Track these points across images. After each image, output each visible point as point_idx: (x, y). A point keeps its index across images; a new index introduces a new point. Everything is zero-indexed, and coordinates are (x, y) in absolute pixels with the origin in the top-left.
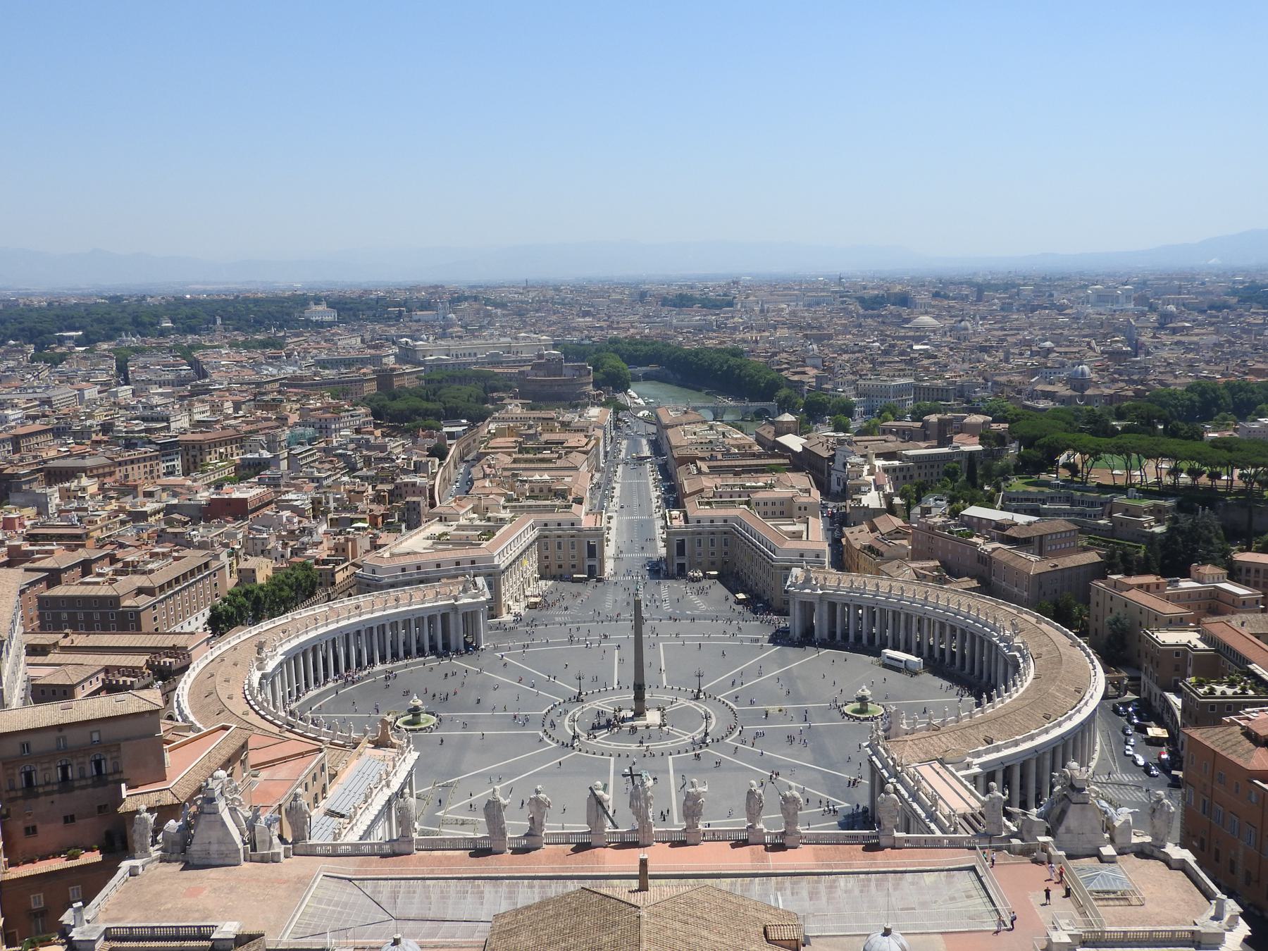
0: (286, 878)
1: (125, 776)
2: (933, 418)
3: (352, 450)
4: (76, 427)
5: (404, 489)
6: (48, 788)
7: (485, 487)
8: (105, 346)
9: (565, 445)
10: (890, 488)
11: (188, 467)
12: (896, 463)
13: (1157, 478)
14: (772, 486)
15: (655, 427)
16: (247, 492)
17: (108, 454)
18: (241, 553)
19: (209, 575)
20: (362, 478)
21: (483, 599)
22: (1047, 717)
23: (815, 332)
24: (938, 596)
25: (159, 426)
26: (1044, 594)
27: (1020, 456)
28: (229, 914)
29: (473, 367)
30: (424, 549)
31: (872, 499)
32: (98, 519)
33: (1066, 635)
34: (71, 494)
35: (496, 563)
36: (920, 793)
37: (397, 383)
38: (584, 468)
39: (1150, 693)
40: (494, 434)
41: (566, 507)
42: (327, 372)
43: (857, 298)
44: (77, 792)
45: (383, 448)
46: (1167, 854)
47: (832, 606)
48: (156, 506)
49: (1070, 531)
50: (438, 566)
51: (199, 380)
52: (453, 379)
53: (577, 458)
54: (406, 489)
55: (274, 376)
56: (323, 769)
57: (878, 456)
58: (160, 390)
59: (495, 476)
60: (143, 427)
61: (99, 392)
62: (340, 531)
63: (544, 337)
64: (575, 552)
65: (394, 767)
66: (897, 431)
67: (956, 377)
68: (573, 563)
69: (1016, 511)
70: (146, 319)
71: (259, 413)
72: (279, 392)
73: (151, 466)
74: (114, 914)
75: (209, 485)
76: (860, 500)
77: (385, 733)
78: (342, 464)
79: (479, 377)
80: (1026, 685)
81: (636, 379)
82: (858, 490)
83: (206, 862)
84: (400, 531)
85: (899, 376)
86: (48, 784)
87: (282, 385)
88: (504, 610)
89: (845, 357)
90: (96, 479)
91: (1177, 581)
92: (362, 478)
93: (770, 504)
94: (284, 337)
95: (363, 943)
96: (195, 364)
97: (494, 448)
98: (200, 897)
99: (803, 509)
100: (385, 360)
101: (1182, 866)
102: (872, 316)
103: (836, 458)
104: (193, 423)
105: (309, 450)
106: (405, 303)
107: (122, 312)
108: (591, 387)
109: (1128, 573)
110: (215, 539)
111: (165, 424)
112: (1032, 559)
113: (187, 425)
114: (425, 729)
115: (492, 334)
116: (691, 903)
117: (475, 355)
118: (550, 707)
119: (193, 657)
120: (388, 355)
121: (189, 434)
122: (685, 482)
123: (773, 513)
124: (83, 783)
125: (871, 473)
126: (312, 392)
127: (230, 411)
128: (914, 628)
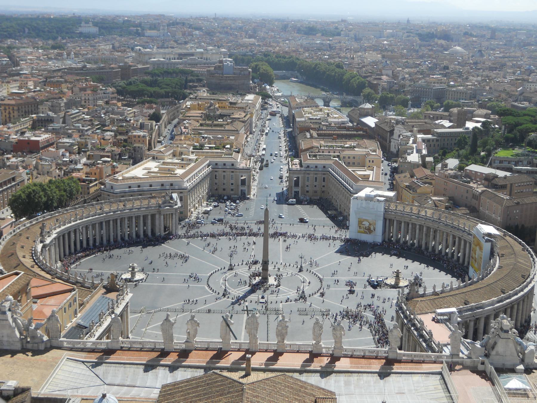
2: (455, 110)
5: (134, 139)
7: (181, 140)
9: (231, 117)
11: (6, 120)
12: (430, 136)
14: (354, 147)
15: (288, 108)
18: (35, 173)
19: (15, 185)
23: (390, 53)
26: (510, 219)
29: (181, 67)
30: (143, 175)
31: (414, 158)
33: (520, 243)
36: (424, 331)
38: (242, 131)
40: (189, 108)
43: (416, 34)
45: (122, 114)
49: (529, 182)
50: (151, 186)
51: (14, 67)
52: (167, 73)
53: (238, 125)
54: (135, 139)
56: (75, 300)
57: (420, 132)
59: (188, 134)
62: (94, 162)
63: (224, 50)
64: (233, 181)
66: (433, 117)
67: (471, 85)
68: (232, 188)
72: (61, 77)
75: (17, 132)
76: (406, 159)
82: (405, 152)
89: (407, 70)
93: (351, 158)
94: (65, 44)
96: (11, 57)
97: (189, 117)
99: (371, 161)
102: (424, 46)
103: (395, 132)
104: (9, 93)
105: (78, 113)
106: (140, 25)
110: (19, 164)
112: (505, 198)
118: (212, 272)
120: (128, 57)
121: (6, 99)
123: (354, 163)
125: (414, 142)
126: (81, 78)
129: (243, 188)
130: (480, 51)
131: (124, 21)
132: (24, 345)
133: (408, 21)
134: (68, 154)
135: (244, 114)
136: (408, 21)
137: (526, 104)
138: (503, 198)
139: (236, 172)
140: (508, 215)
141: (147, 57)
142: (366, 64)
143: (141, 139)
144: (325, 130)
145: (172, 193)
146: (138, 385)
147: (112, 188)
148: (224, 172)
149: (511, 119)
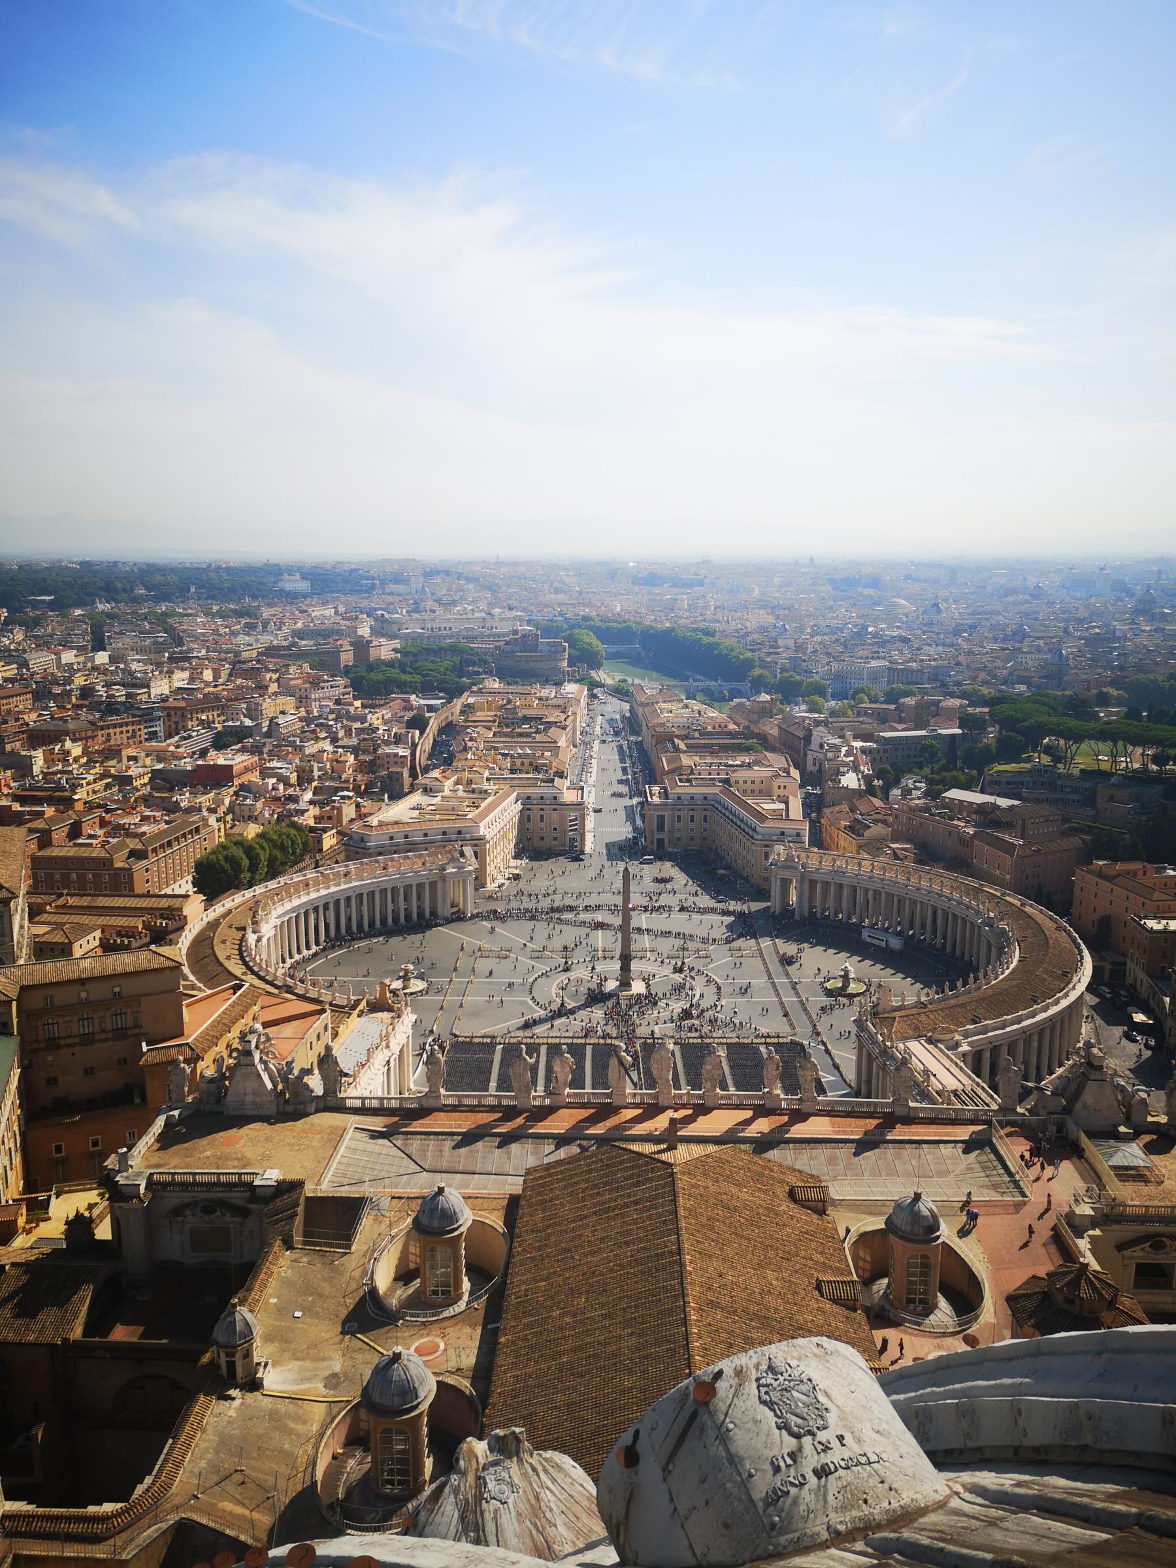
0: (319, 1128)
2: (909, 701)
3: (332, 720)
4: (57, 690)
5: (386, 760)
8: (78, 612)
10: (869, 770)
13: (1143, 764)
16: (234, 759)
17: (91, 718)
21: (471, 868)
24: (920, 876)
25: (139, 692)
27: (999, 740)
31: (850, 780)
32: (84, 782)
34: (56, 757)
35: (481, 834)
37: (373, 653)
38: (562, 743)
39: (1136, 979)
41: (548, 781)
42: (304, 642)
43: (828, 580)
44: (98, 1045)
45: (363, 720)
47: (813, 883)
48: (141, 770)
50: (426, 835)
52: (428, 651)
54: (388, 759)
55: (251, 645)
57: (855, 737)
60: (124, 693)
65: (393, 1029)
68: (555, 835)
69: (999, 795)
70: (119, 585)
71: (239, 681)
72: (258, 662)
73: (133, 730)
74: (154, 1160)
79: (454, 650)
80: (1012, 967)
83: (239, 1112)
84: (383, 800)
85: (873, 658)
86: (70, 1036)
88: (488, 879)
90: (80, 743)
91: (1165, 868)
92: (343, 747)
93: (749, 782)
95: (399, 1193)
97: (475, 722)
98: (238, 1146)
99: (782, 787)
100: (360, 632)
107: (95, 577)
108: (565, 663)
109: (1115, 859)
111: (146, 690)
112: (1015, 842)
113: (167, 692)
114: (415, 993)
117: (450, 629)
121: (171, 700)
122: (664, 759)
123: (753, 791)
124: (104, 1036)
125: (847, 755)
128: (895, 908)
130: (936, 605)
132: (281, 1107)
133: (811, 560)
134: (281, 787)
135: (563, 716)
136: (811, 560)
137: (1023, 688)
138: (1012, 843)
139: (561, 810)
141: (395, 627)
142: (749, 630)
144: (698, 738)
145: (462, 846)
146: (478, 1170)
147: (362, 840)
148: (542, 809)
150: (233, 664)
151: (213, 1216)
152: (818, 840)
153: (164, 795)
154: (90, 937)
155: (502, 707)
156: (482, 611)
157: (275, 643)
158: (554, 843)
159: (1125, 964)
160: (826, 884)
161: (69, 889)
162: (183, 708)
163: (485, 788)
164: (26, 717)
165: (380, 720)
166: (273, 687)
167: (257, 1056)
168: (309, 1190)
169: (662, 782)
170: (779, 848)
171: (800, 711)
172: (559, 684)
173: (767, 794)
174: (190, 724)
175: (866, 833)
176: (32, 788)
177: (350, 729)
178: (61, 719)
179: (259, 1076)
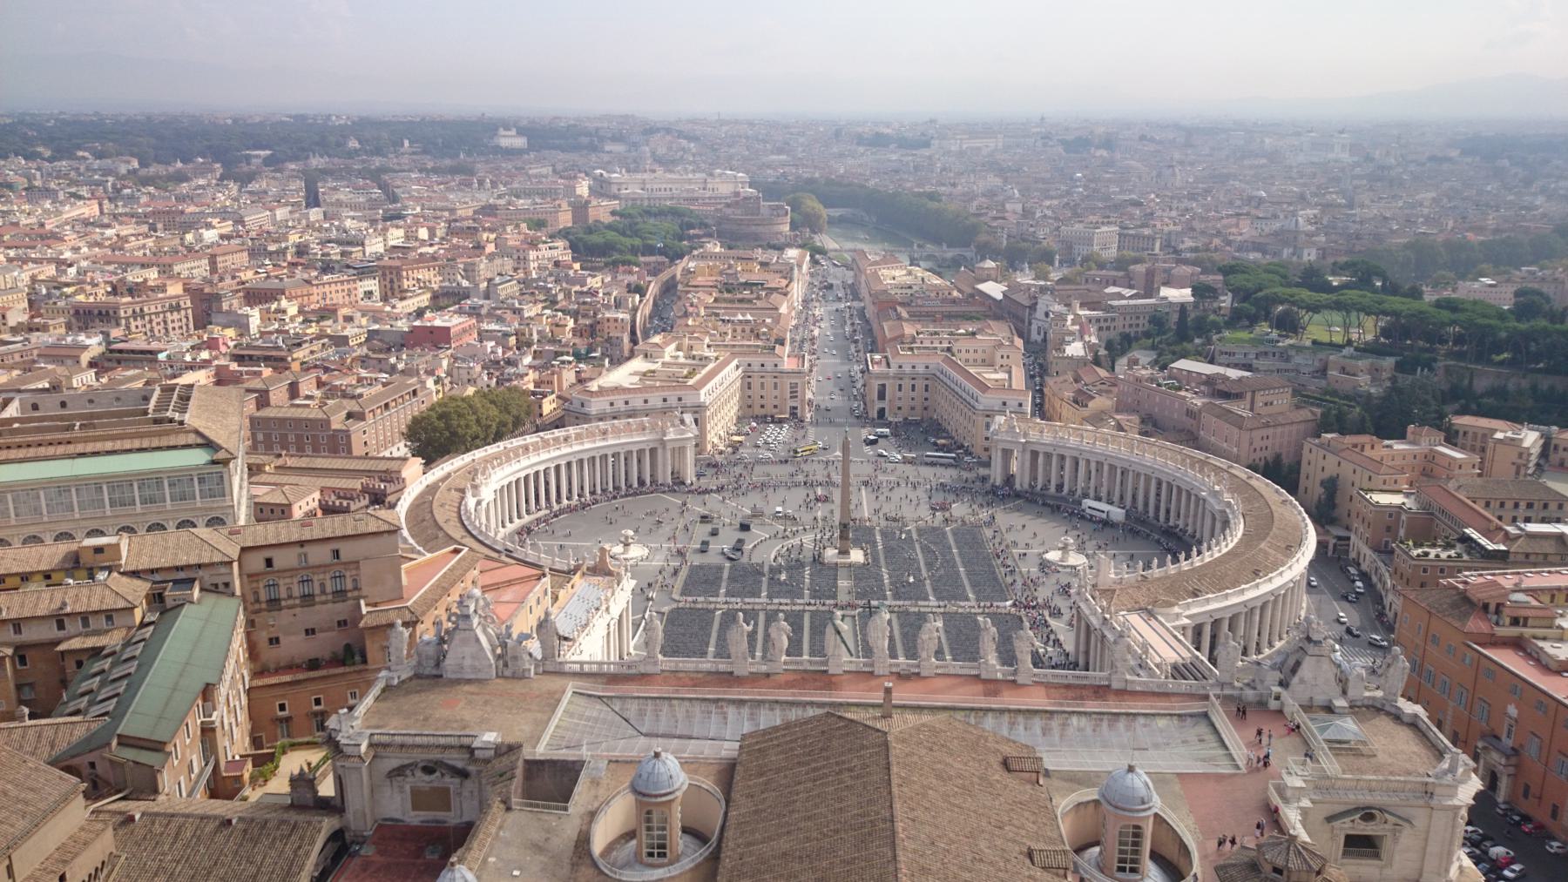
1: (364, 594)
2: (1140, 269)
4: (272, 248)
5: (606, 325)
6: (290, 602)
7: (687, 325)
8: (293, 167)
17: (306, 276)
18: (447, 381)
20: (563, 311)
21: (690, 435)
22: (1256, 574)
27: (1233, 309)
28: (486, 724)
29: (668, 203)
31: (1075, 349)
33: (1277, 491)
38: (783, 309)
39: (1359, 554)
42: (521, 201)
44: (318, 607)
46: (1399, 708)
47: (1035, 454)
48: (356, 330)
57: (1082, 305)
58: (352, 214)
61: (291, 212)
64: (776, 393)
71: (455, 240)
72: (474, 220)
73: (349, 290)
74: (374, 722)
77: (603, 559)
78: (542, 297)
79: (674, 212)
81: (832, 222)
85: (1103, 223)
86: (290, 597)
87: (475, 212)
100: (578, 191)
101: (1413, 724)
108: (787, 228)
109: (1342, 432)
113: (382, 250)
115: (686, 169)
116: (933, 730)
119: (408, 482)
123: (975, 360)
127: (426, 237)
129: (794, 404)
131: (569, 126)
133: (1043, 119)
134: (500, 351)
140: (1251, 444)
141: (614, 189)
143: (619, 325)
146: (695, 735)
149: (1238, 280)
150: (449, 222)
151: (433, 777)
152: (1040, 410)
153: (381, 356)
154: (309, 499)
155: (721, 273)
156: (703, 171)
157: (491, 201)
158: (775, 411)
159: (1348, 539)
160: (1048, 456)
161: (288, 450)
162: (398, 267)
163: (706, 354)
164: (242, 274)
165: (599, 284)
166: (490, 248)
167: (475, 621)
168: (527, 753)
169: (884, 351)
170: (1000, 419)
171: (1025, 278)
172: (780, 248)
173: (988, 363)
174: (406, 284)
175: (1091, 404)
176: (249, 347)
177: (570, 293)
178: (276, 277)
179: (478, 640)
